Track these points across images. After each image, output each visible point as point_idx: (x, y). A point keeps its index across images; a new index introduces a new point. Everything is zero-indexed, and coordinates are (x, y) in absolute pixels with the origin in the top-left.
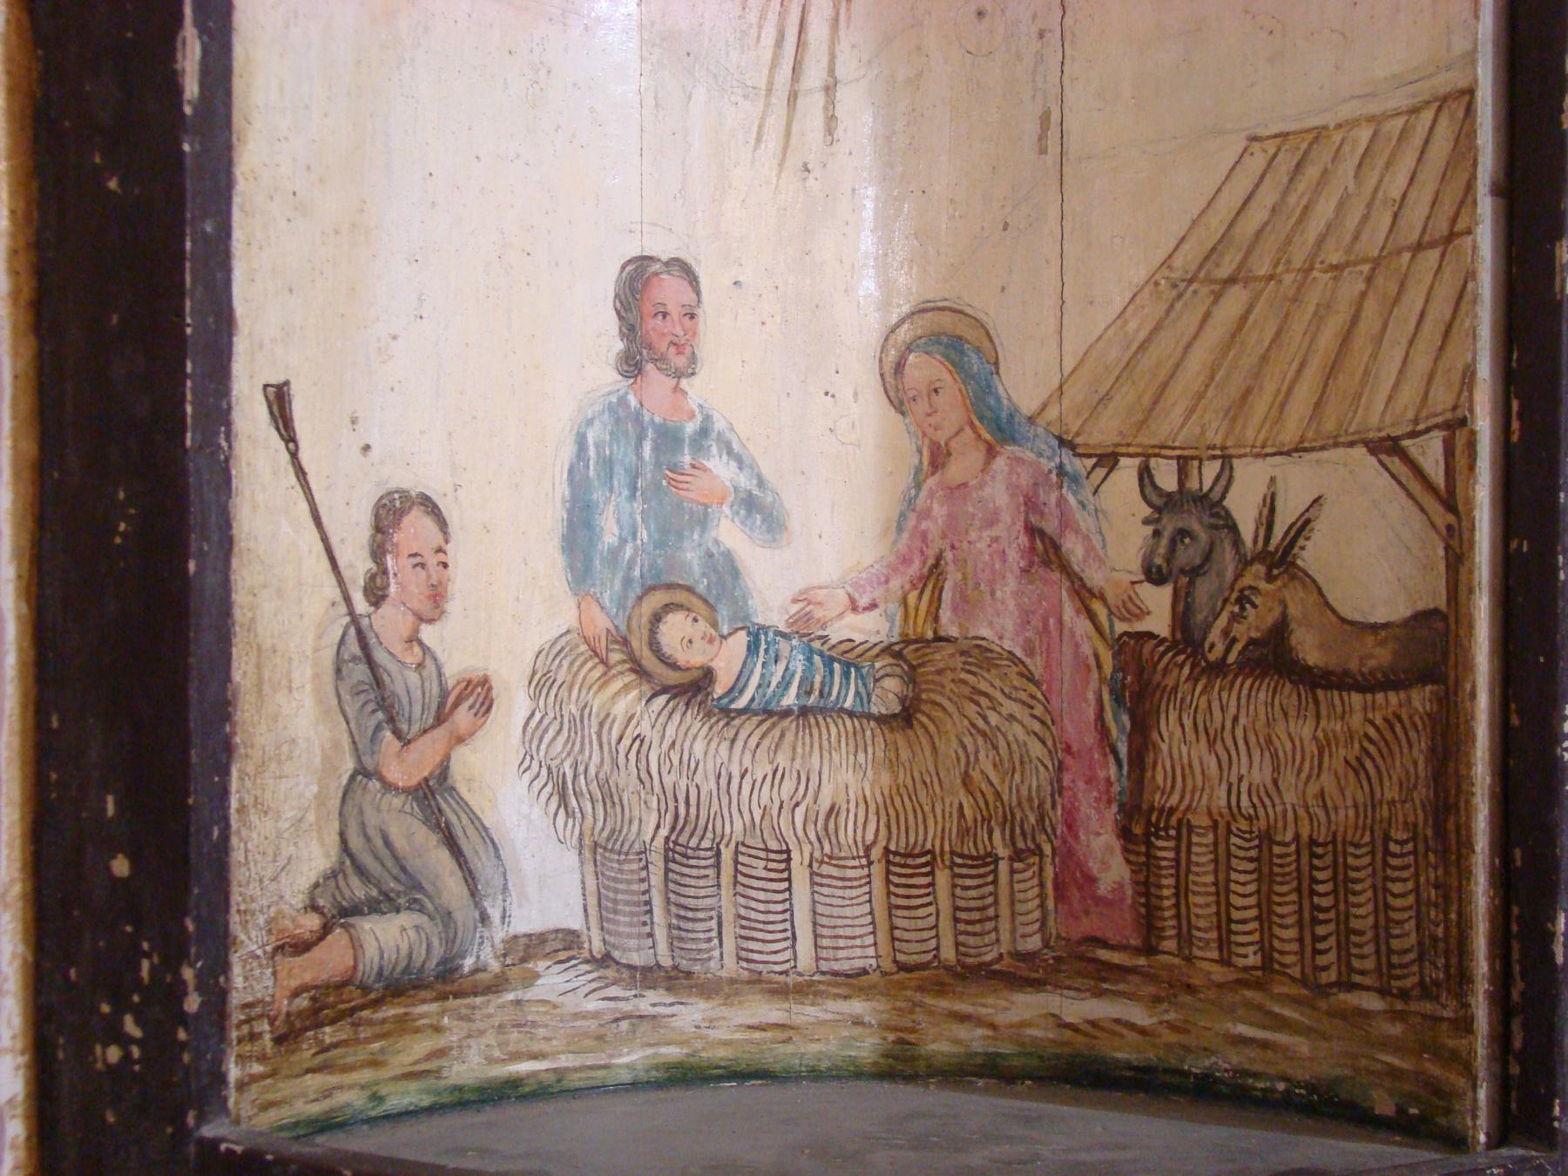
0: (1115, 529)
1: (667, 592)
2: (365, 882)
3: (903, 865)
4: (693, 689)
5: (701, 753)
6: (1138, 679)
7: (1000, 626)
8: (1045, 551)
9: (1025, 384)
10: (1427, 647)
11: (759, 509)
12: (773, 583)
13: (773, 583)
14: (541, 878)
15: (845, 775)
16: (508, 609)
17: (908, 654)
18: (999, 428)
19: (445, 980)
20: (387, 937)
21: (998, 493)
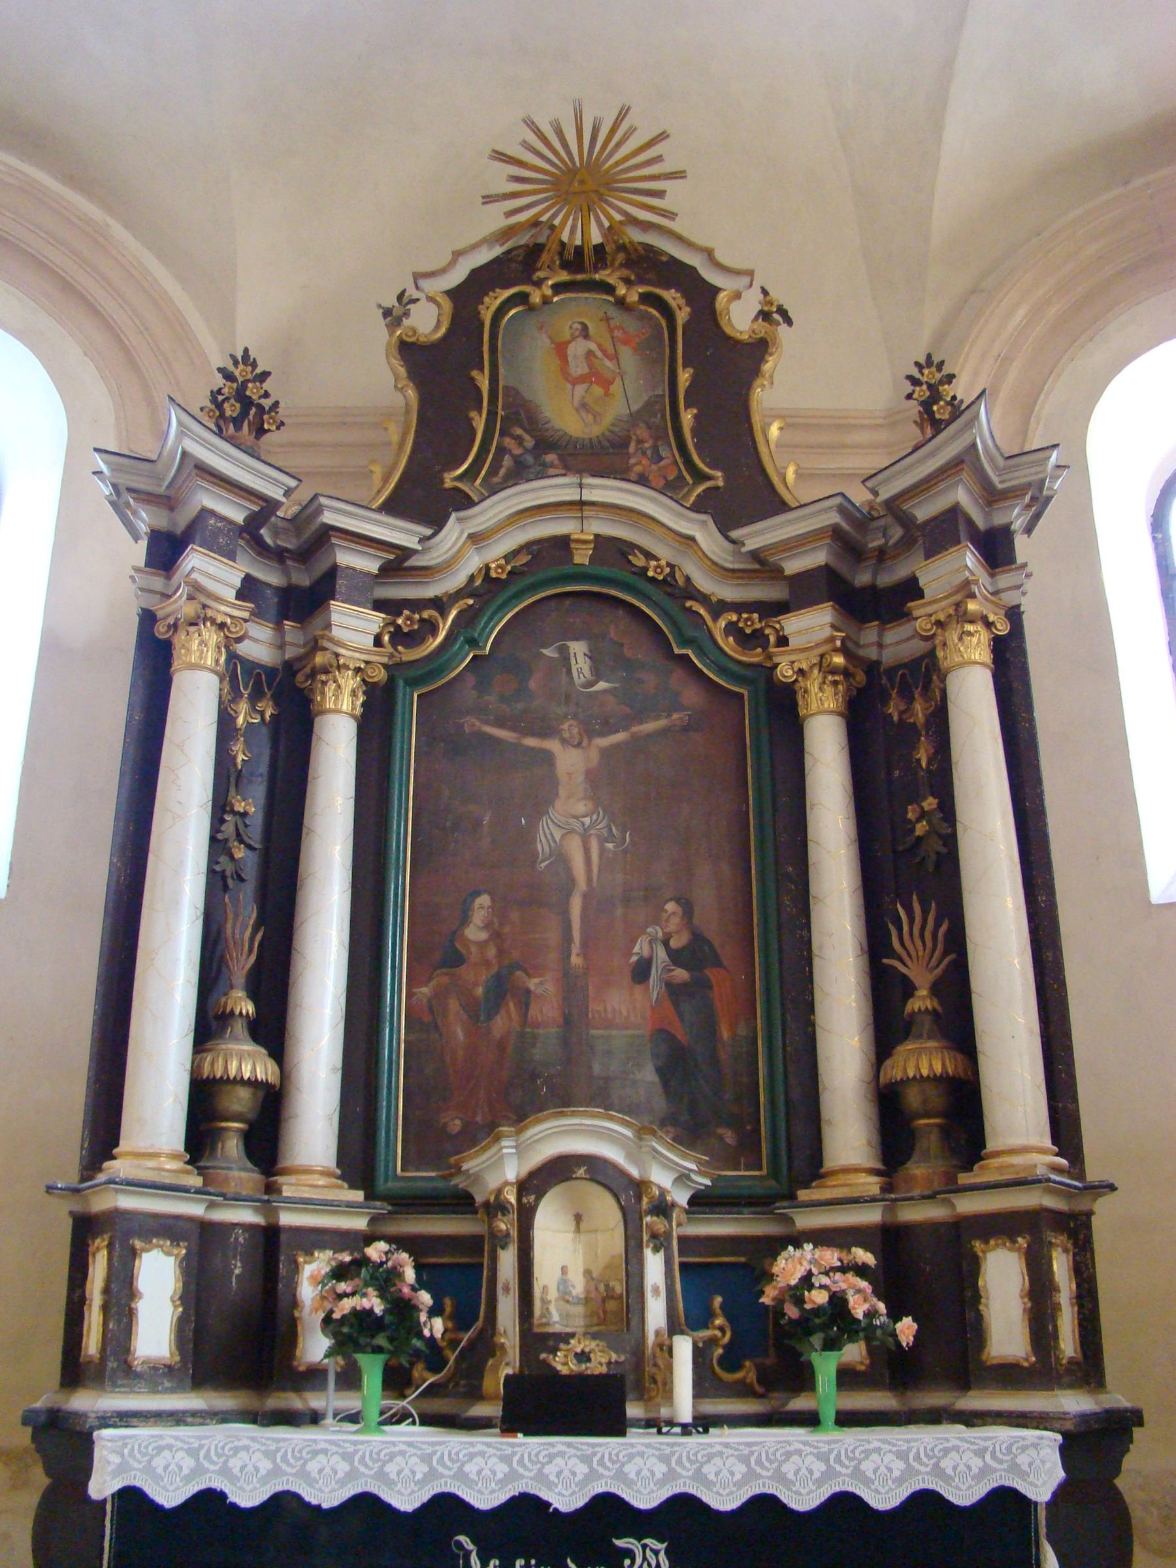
0: (602, 1287)
1: (565, 1293)
2: (542, 1316)
3: (586, 1317)
4: (568, 1301)
5: (568, 1307)
6: (604, 1300)
7: (593, 1295)
8: (597, 1289)
9: (594, 1275)
10: (621, 1295)
11: (573, 1286)
12: (574, 1292)
13: (574, 1292)
14: (556, 1317)
15: (580, 1310)
16: (553, 1294)
17: (586, 1298)
18: (593, 1279)
19: (547, 1324)
20: (544, 1320)
21: (592, 1284)
